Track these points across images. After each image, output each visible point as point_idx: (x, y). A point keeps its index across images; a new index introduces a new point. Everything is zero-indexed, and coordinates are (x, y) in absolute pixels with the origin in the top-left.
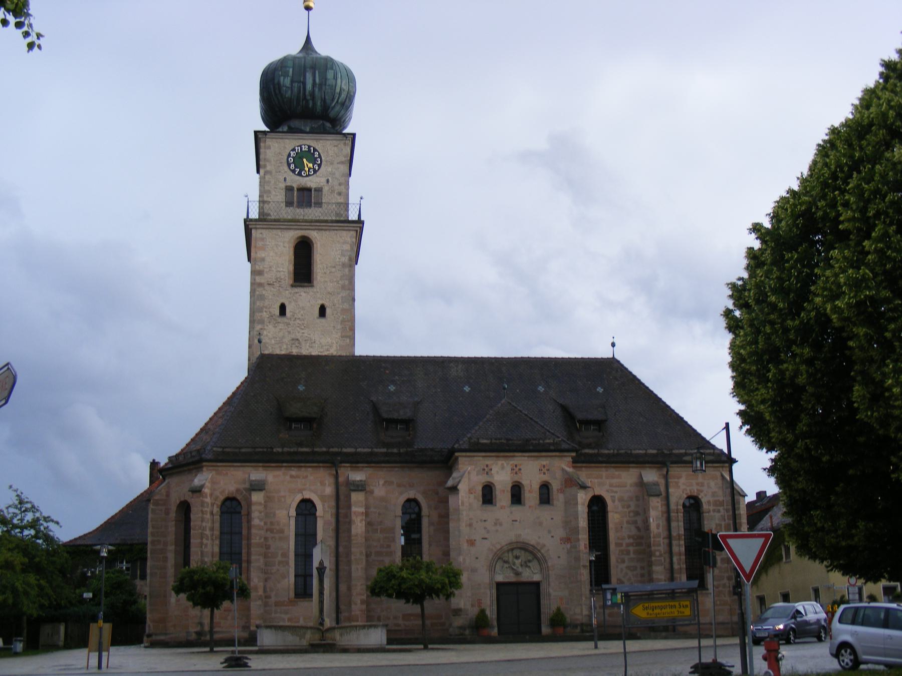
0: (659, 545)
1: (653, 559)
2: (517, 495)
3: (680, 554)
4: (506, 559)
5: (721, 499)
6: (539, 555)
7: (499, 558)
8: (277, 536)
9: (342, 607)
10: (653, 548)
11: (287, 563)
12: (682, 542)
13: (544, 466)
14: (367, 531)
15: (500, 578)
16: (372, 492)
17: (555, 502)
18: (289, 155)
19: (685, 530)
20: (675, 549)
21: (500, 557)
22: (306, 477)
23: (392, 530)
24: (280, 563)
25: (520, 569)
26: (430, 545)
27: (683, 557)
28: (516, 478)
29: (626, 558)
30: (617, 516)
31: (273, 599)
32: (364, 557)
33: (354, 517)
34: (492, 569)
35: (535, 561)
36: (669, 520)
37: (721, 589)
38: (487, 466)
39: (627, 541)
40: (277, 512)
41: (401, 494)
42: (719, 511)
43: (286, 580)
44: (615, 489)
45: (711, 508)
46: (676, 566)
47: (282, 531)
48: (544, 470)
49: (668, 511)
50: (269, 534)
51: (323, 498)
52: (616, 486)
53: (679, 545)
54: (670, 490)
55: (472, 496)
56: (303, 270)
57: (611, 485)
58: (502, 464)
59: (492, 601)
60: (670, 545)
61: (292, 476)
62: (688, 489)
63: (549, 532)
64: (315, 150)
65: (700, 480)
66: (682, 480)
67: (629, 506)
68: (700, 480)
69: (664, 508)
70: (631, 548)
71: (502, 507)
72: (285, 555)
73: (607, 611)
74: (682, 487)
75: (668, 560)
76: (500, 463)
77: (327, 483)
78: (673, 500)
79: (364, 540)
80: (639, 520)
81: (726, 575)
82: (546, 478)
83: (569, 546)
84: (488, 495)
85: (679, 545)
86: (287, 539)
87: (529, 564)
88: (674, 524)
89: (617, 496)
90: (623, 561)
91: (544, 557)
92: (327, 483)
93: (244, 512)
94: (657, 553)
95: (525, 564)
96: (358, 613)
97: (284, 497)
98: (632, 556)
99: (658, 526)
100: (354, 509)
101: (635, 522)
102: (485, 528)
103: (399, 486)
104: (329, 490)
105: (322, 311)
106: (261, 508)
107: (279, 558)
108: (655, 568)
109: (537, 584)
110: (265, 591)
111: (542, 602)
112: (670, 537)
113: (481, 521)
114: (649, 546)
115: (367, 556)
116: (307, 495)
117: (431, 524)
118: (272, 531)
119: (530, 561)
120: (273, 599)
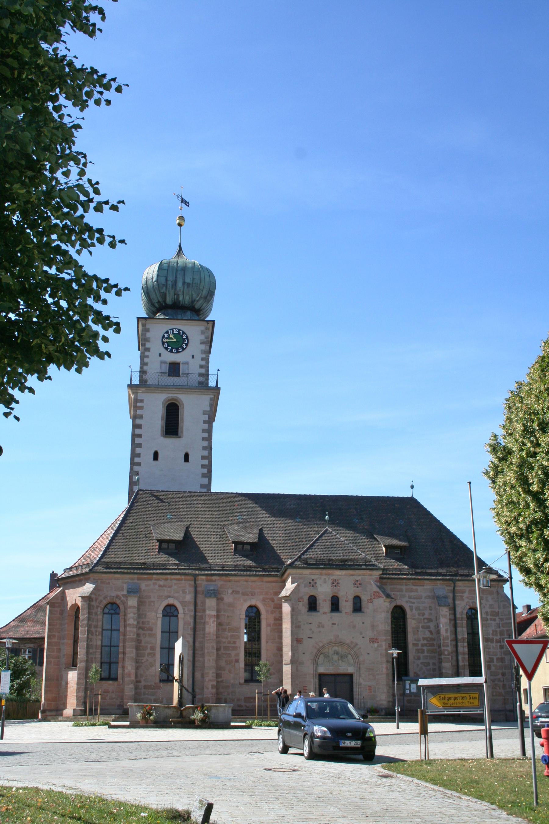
0: (448, 646)
1: (443, 657)
3: (464, 654)
5: (497, 610)
8: (147, 632)
9: (197, 690)
10: (442, 648)
12: (466, 644)
13: (357, 581)
14: (218, 630)
15: (321, 670)
16: (222, 599)
18: (164, 336)
19: (468, 634)
20: (460, 649)
23: (238, 629)
24: (149, 654)
26: (267, 642)
27: (466, 656)
29: (421, 655)
31: (143, 683)
32: (215, 651)
33: (207, 619)
34: (315, 663)
36: (455, 626)
37: (496, 682)
38: (313, 580)
40: (148, 614)
41: (245, 601)
42: (495, 620)
43: (153, 668)
46: (461, 663)
47: (151, 629)
48: (358, 584)
49: (455, 619)
50: (141, 631)
51: (183, 603)
52: (414, 598)
54: (457, 602)
55: (301, 604)
56: (172, 425)
57: (410, 597)
58: (325, 579)
60: (456, 646)
61: (160, 586)
62: (471, 601)
63: (361, 633)
64: (184, 333)
69: (452, 617)
70: (425, 648)
71: (324, 613)
72: (153, 648)
73: (406, 698)
74: (466, 600)
75: (455, 658)
76: (323, 577)
78: (458, 610)
79: (215, 637)
80: (432, 625)
81: (500, 671)
82: (358, 591)
85: (464, 647)
86: (153, 636)
88: (459, 629)
89: (414, 605)
90: (419, 658)
93: (122, 613)
94: (446, 653)
96: (210, 696)
97: (154, 602)
98: (426, 654)
99: (447, 630)
100: (208, 612)
101: (429, 627)
102: (311, 629)
104: (189, 597)
105: (186, 458)
106: (135, 610)
107: (149, 651)
108: (444, 664)
109: (351, 676)
110: (136, 676)
111: (355, 690)
112: (456, 640)
113: (307, 623)
114: (440, 647)
115: (218, 649)
116: (171, 601)
117: (268, 625)
118: (143, 629)
120: (143, 683)
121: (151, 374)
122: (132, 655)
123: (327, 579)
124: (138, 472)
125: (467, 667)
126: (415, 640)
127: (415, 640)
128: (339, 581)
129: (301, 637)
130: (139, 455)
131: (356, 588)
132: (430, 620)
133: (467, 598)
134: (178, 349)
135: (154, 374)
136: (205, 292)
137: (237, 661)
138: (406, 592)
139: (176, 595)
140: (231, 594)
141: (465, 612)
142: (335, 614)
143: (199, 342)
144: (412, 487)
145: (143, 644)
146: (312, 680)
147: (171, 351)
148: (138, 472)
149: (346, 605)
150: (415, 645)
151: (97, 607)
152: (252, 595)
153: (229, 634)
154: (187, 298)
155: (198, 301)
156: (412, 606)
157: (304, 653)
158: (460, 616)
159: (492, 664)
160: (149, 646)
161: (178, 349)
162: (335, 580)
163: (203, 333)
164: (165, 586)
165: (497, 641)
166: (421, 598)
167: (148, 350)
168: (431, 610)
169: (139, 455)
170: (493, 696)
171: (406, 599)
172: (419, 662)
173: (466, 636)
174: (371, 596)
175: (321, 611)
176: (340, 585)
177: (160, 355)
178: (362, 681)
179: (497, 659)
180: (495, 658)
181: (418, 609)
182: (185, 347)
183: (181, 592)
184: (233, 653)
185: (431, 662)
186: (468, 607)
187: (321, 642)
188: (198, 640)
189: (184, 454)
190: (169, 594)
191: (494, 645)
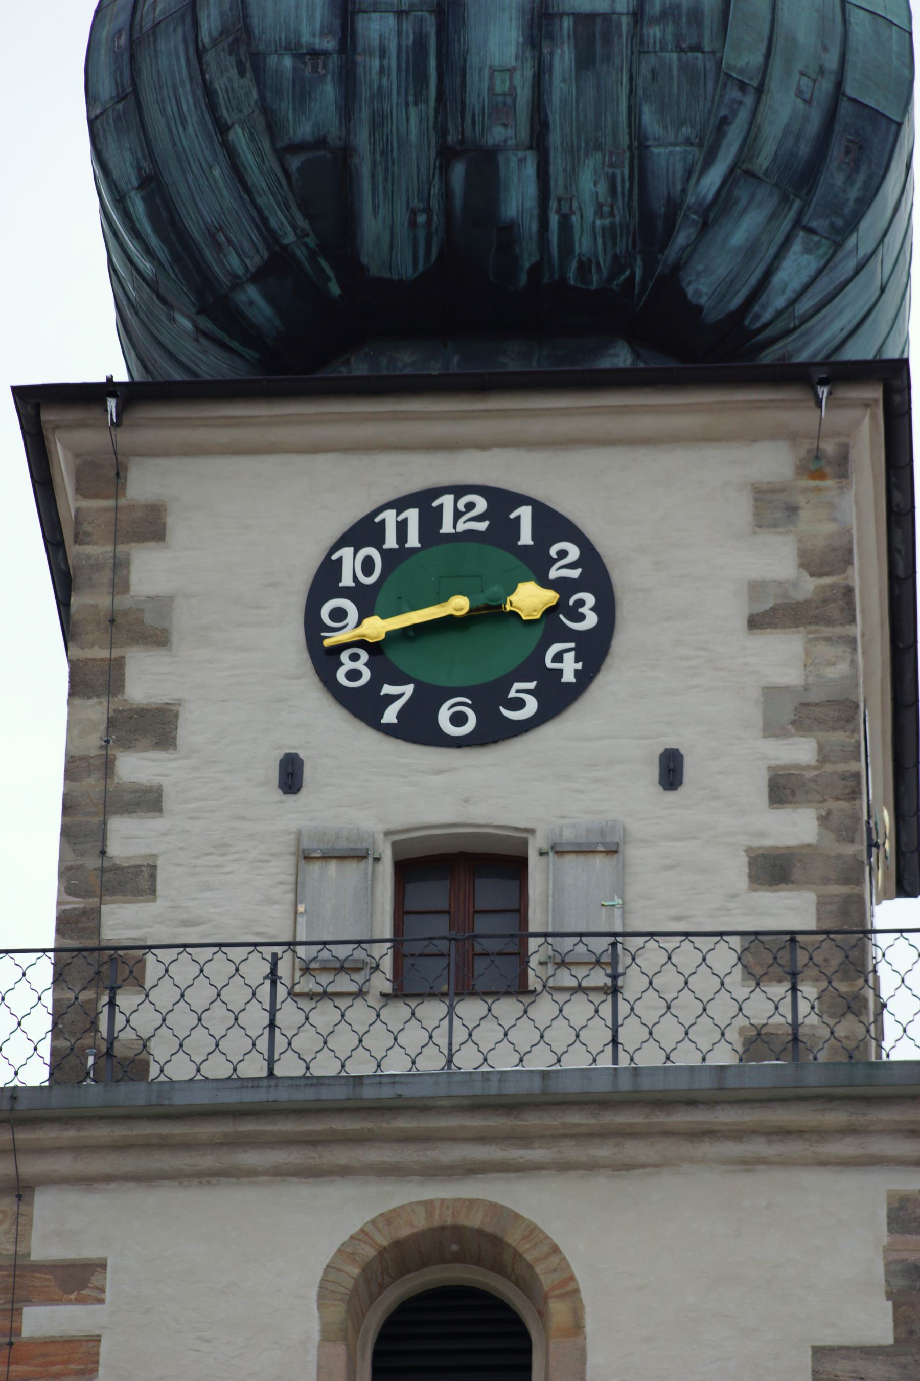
64: (552, 524)
121: (184, 970)
134: (489, 697)
135: (219, 968)
136: (786, 112)
143: (736, 611)
147: (418, 728)
154: (589, 184)
155: (714, 213)
161: (489, 697)
163: (772, 508)
167: (155, 727)
177: (291, 776)
182: (569, 668)
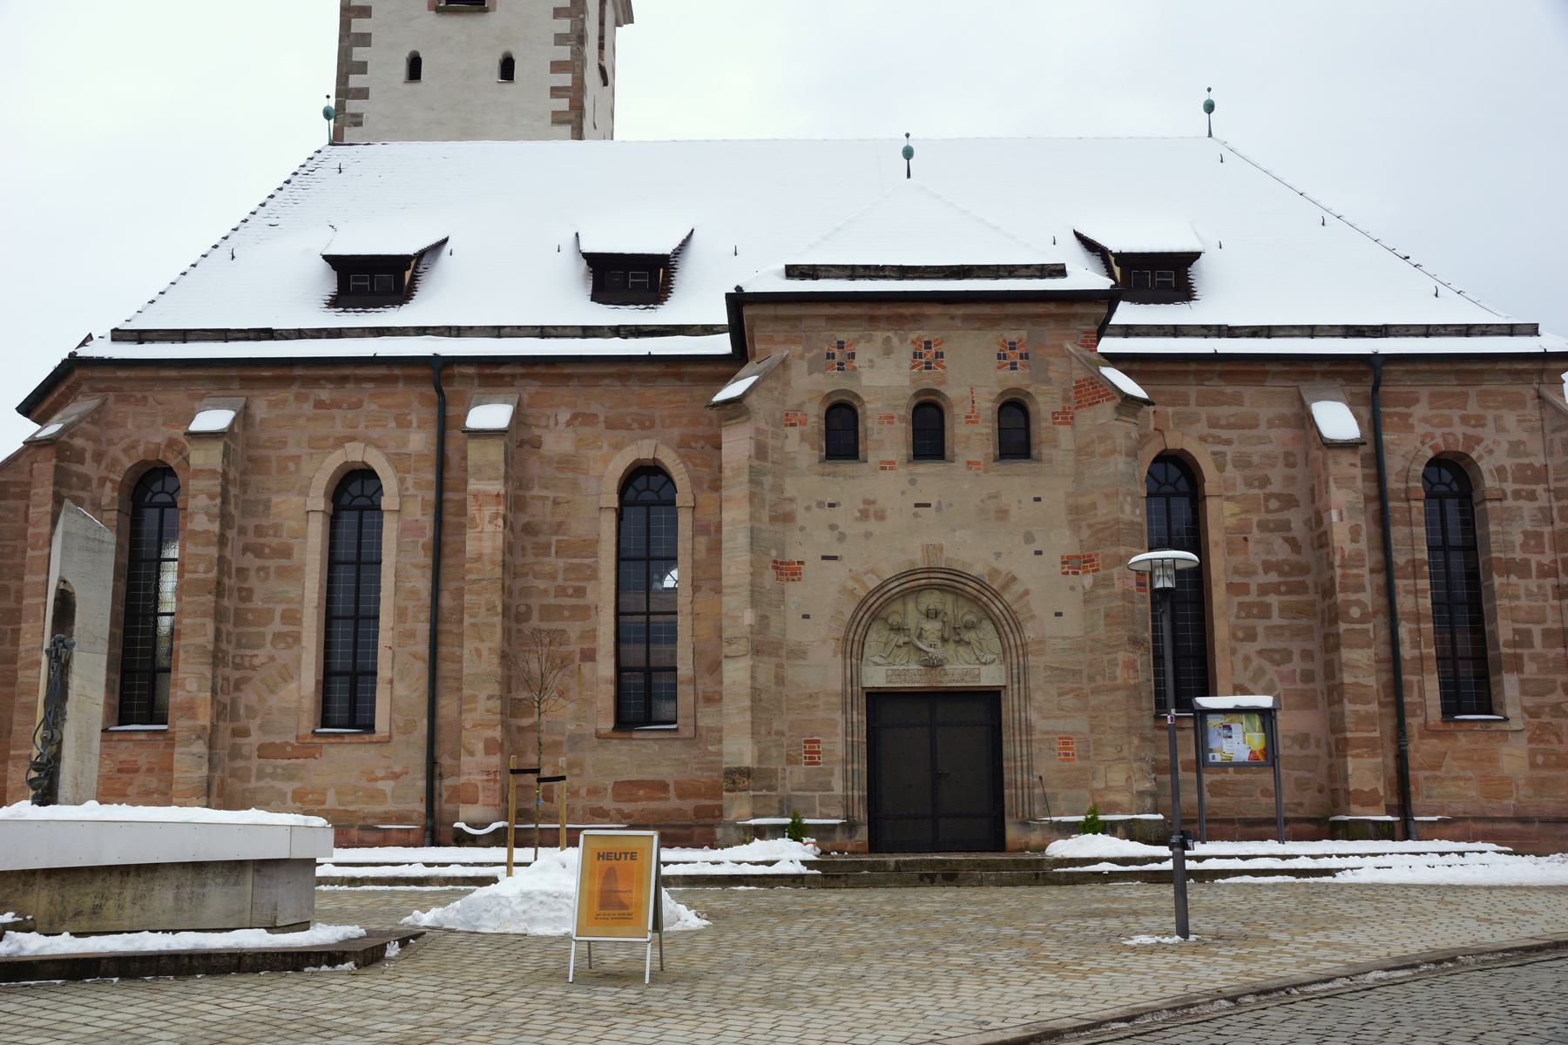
0: (1360, 588)
1: (1342, 626)
2: (929, 432)
4: (895, 619)
5: (1538, 461)
6: (997, 608)
7: (874, 617)
8: (271, 564)
10: (1340, 597)
11: (297, 638)
12: (1425, 584)
13: (1013, 346)
14: (509, 548)
15: (877, 677)
17: (1046, 451)
19: (1430, 549)
20: (1404, 602)
21: (875, 610)
22: (359, 405)
23: (589, 546)
24: (278, 636)
25: (938, 652)
27: (1428, 626)
28: (928, 381)
29: (1260, 625)
30: (1230, 508)
31: (255, 739)
32: (498, 620)
33: (472, 509)
35: (987, 626)
36: (1383, 520)
37: (1545, 719)
38: (841, 345)
39: (1262, 578)
40: (275, 499)
41: (617, 447)
42: (1532, 496)
43: (293, 686)
44: (1224, 434)
45: (1509, 487)
46: (1407, 652)
47: (286, 552)
48: (1013, 356)
49: (1382, 496)
51: (399, 461)
52: (1230, 426)
53: (1416, 592)
54: (1387, 437)
55: (794, 433)
57: (1213, 423)
58: (888, 340)
59: (851, 747)
60: (1389, 591)
61: (319, 404)
63: (1029, 538)
65: (1473, 408)
66: (1420, 410)
67: (1265, 482)
68: (1473, 408)
69: (1372, 489)
70: (1273, 600)
71: (885, 466)
72: (292, 617)
73: (1207, 778)
74: (1421, 429)
75: (1384, 633)
76: (879, 335)
77: (414, 419)
78: (1394, 464)
79: (498, 572)
80: (1297, 519)
82: (1016, 379)
83: (1088, 580)
84: (842, 432)
85: (1416, 592)
87: (970, 636)
88: (1397, 532)
90: (1251, 636)
91: (1013, 614)
92: (414, 419)
94: (1355, 612)
95: (955, 635)
96: (478, 778)
97: (296, 459)
98: (1276, 620)
99: (1355, 534)
100: (474, 485)
101: (1284, 526)
102: (833, 527)
103: (611, 425)
104: (420, 441)
105: (507, 69)
106: (215, 485)
107: (277, 626)
109: (991, 698)
111: (1007, 750)
112: (1387, 568)
113: (820, 505)
114: (1328, 591)
116: (356, 453)
119: (969, 627)
120: (255, 739)
122: (200, 640)
123: (895, 341)
124: (360, 116)
125: (1433, 664)
126: (1236, 571)
127: (1236, 571)
128: (943, 348)
129: (793, 555)
130: (362, 68)
131: (1006, 372)
132: (1289, 502)
133: (1425, 420)
137: (589, 655)
138: (1198, 405)
139: (375, 433)
140: (568, 424)
141: (1421, 469)
142: (925, 468)
144: (1209, 107)
145: (257, 603)
146: (838, 716)
148: (360, 116)
149: (972, 434)
150: (1233, 588)
151: (102, 482)
152: (643, 427)
153: (561, 563)
156: (1224, 454)
157: (806, 617)
158: (1403, 486)
159: (1526, 652)
160: (279, 609)
162: (928, 344)
164: (335, 404)
165: (1544, 573)
166: (1256, 426)
168: (1293, 465)
169: (362, 68)
170: (1533, 765)
171: (1202, 428)
172: (1251, 648)
173: (1423, 555)
174: (1066, 399)
175: (873, 459)
176: (945, 361)
178: (1034, 717)
179: (1547, 634)
180: (1537, 630)
181: (1242, 463)
183: (393, 424)
184: (574, 629)
185: (1296, 647)
186: (1430, 454)
187: (872, 571)
188: (448, 586)
189: (498, 57)
190: (348, 432)
191: (1533, 584)
